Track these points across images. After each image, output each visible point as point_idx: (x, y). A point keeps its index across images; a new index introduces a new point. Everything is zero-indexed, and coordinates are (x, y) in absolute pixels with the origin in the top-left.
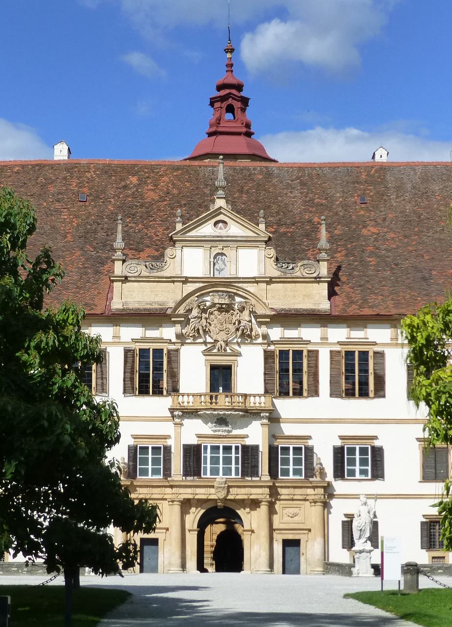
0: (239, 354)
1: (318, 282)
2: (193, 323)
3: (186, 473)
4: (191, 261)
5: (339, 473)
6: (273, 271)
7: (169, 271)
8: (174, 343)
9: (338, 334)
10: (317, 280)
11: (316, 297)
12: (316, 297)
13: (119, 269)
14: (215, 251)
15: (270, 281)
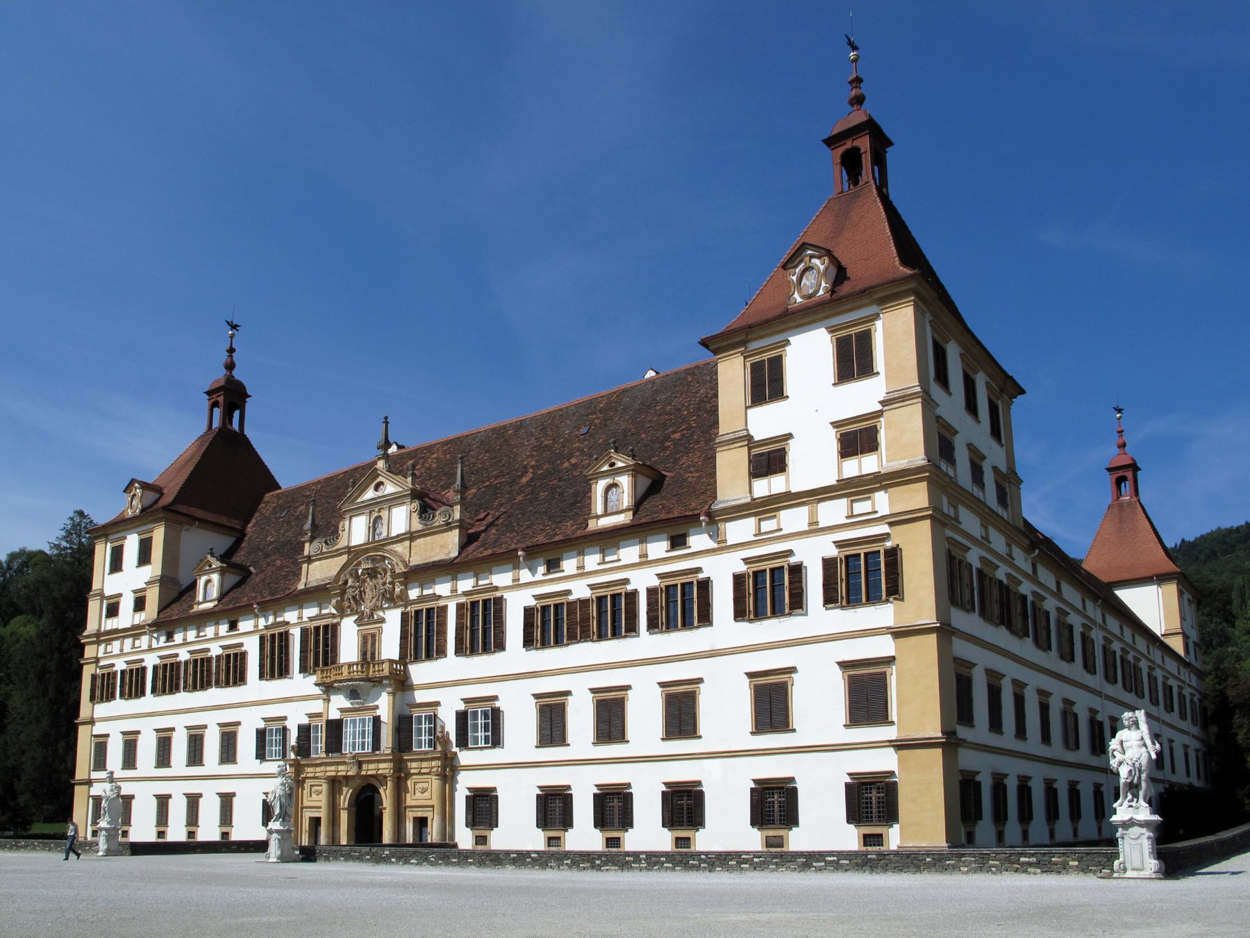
0: (382, 621)
1: (451, 529)
2: (350, 593)
3: (328, 750)
4: (357, 531)
5: (463, 742)
6: (417, 526)
7: (342, 543)
8: (333, 616)
9: (466, 584)
10: (448, 527)
11: (447, 545)
12: (447, 545)
13: (307, 549)
14: (375, 515)
15: (411, 536)
